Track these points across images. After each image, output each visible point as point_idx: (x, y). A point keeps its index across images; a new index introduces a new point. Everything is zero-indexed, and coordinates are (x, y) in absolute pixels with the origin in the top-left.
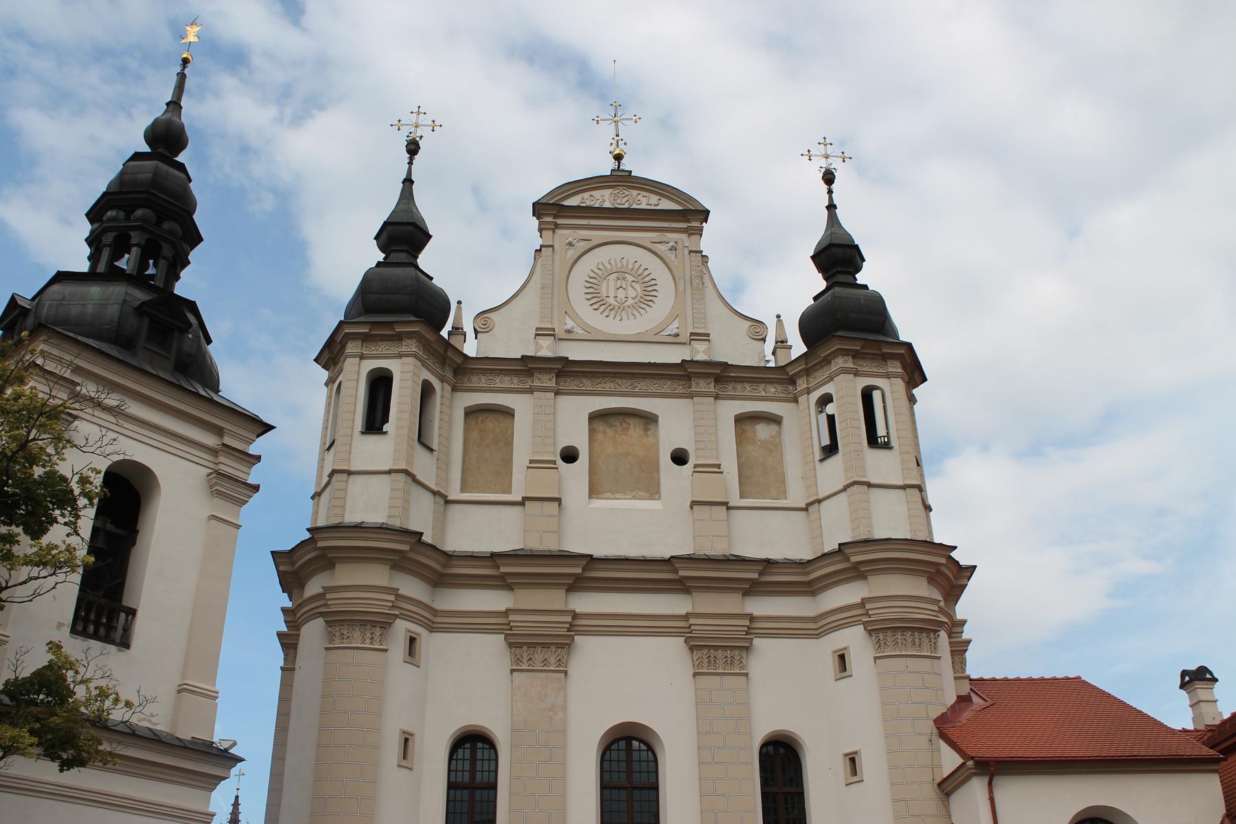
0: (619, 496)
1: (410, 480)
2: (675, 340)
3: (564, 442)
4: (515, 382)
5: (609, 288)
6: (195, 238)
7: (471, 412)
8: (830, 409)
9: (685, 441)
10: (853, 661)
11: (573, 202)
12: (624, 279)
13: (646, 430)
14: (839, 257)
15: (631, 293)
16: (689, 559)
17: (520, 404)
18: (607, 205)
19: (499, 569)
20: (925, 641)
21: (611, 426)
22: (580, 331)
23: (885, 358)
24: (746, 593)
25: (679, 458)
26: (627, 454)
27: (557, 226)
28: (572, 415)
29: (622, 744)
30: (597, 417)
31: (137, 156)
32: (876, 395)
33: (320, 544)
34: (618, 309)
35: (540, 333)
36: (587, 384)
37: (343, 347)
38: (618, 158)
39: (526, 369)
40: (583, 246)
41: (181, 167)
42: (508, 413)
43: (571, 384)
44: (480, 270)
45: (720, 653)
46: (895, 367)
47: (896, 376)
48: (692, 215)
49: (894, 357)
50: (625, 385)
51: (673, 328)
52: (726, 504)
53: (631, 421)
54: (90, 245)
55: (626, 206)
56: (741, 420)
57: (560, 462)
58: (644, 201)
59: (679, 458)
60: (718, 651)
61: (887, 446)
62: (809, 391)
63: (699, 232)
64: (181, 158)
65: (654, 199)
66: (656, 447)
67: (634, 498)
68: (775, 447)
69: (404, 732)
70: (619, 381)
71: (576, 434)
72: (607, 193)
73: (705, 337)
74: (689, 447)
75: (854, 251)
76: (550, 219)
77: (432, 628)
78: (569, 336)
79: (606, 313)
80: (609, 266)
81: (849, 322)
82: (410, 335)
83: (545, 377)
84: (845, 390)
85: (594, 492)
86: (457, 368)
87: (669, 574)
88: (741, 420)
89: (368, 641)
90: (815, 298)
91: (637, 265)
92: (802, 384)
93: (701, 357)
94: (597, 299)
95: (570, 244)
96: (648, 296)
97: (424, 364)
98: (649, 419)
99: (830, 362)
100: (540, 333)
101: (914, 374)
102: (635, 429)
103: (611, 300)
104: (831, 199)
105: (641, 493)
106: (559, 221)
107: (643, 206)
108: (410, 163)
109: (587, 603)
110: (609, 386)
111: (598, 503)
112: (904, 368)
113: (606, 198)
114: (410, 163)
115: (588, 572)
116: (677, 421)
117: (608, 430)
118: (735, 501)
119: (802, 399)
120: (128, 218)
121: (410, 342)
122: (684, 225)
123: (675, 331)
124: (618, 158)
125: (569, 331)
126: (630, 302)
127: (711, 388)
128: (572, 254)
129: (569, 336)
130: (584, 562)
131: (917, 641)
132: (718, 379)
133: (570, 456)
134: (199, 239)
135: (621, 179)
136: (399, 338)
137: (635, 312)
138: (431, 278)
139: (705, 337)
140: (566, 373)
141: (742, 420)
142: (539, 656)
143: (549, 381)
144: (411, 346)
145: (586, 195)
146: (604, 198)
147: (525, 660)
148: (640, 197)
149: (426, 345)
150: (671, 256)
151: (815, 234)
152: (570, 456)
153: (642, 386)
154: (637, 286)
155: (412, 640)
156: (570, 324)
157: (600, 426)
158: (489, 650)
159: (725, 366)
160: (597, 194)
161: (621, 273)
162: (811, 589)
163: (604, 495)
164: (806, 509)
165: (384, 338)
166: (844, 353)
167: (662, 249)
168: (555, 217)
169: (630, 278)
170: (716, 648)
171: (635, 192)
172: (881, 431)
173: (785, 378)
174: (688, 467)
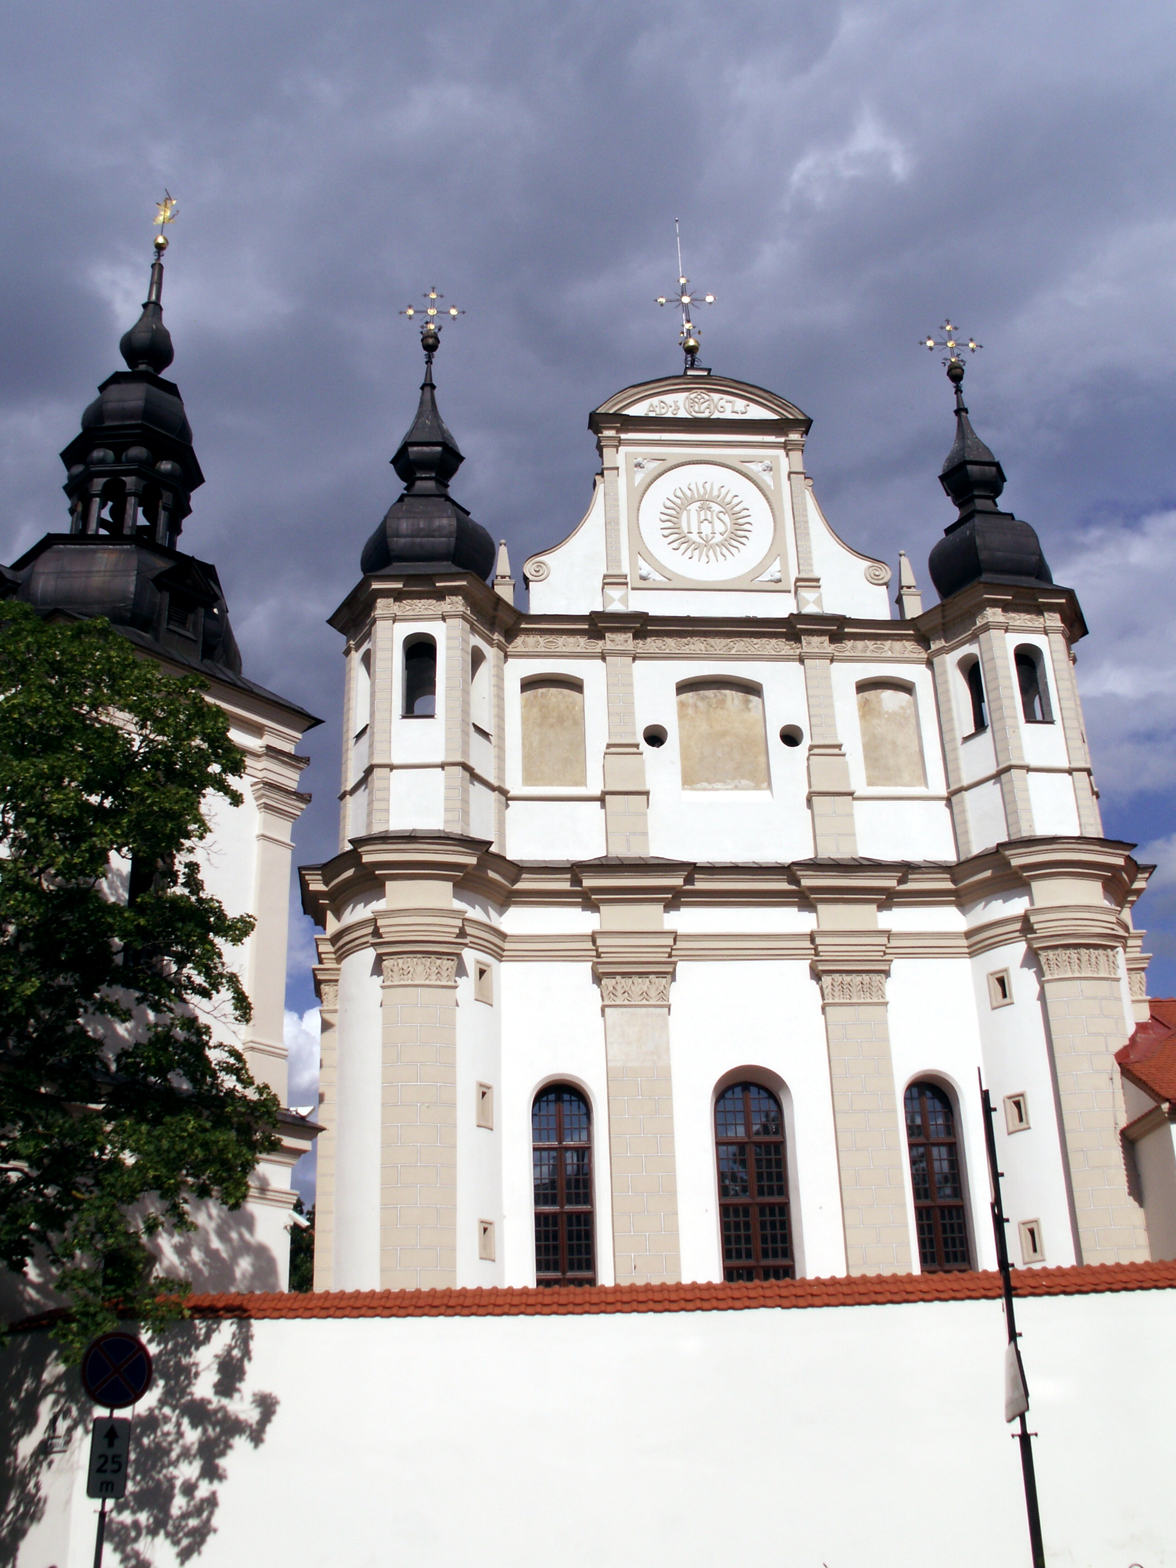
0: (719, 785)
1: (467, 775)
2: (776, 586)
4: (582, 643)
5: (691, 520)
7: (529, 684)
12: (709, 508)
15: (719, 527)
16: (814, 865)
17: (591, 672)
18: (682, 414)
19: (581, 882)
20: (1102, 959)
21: (703, 699)
22: (658, 577)
23: (1039, 610)
25: (791, 737)
26: (724, 734)
27: (620, 442)
28: (653, 684)
30: (684, 687)
31: (117, 378)
33: (366, 859)
35: (611, 581)
36: (671, 644)
37: (371, 606)
40: (652, 466)
41: (171, 389)
42: (575, 685)
43: (651, 645)
45: (857, 979)
46: (1054, 620)
47: (1055, 631)
49: (1052, 608)
50: (719, 644)
51: (774, 570)
52: (851, 794)
55: (706, 415)
56: (864, 686)
57: (644, 746)
58: (728, 407)
59: (791, 737)
60: (847, 975)
64: (166, 375)
69: (481, 1085)
70: (710, 640)
72: (681, 397)
74: (802, 722)
75: (994, 469)
76: (611, 433)
77: (499, 957)
78: (644, 585)
79: (689, 553)
80: (689, 493)
82: (454, 591)
83: (620, 637)
85: (689, 780)
89: (434, 977)
90: (948, 531)
91: (724, 491)
93: (810, 609)
94: (676, 533)
95: (638, 465)
96: (738, 531)
97: (473, 630)
98: (751, 689)
100: (611, 581)
101: (1075, 626)
102: (732, 696)
103: (694, 536)
104: (959, 401)
105: (744, 782)
106: (623, 436)
108: (429, 362)
109: (688, 920)
110: (697, 645)
112: (1063, 621)
113: (681, 404)
114: (429, 362)
115: (687, 883)
117: (700, 704)
120: (118, 460)
121: (454, 598)
122: (782, 440)
123: (778, 576)
126: (718, 538)
127: (829, 648)
128: (640, 476)
131: (1093, 960)
133: (655, 737)
134: (202, 481)
136: (440, 595)
137: (725, 551)
138: (468, 513)
139: (813, 583)
143: (622, 641)
144: (456, 604)
145: (655, 401)
147: (619, 993)
148: (722, 403)
149: (470, 601)
150: (767, 478)
152: (655, 737)
153: (740, 645)
154: (726, 518)
155: (482, 972)
157: (689, 697)
159: (842, 621)
161: (705, 501)
163: (699, 786)
165: (420, 596)
166: (994, 603)
167: (755, 468)
169: (716, 508)
171: (716, 396)
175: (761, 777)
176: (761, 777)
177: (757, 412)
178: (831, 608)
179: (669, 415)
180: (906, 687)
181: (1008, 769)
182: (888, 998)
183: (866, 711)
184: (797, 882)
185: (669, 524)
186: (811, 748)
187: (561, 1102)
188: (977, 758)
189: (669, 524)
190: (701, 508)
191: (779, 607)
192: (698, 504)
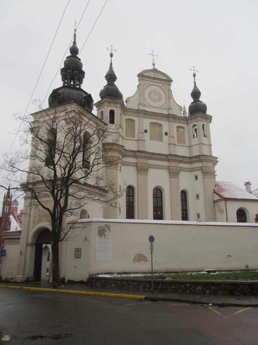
0: (155, 140)
2: (165, 109)
3: (145, 128)
5: (153, 95)
6: (83, 73)
7: (126, 120)
8: (195, 127)
9: (167, 131)
10: (199, 177)
11: (146, 74)
13: (160, 127)
14: (196, 94)
15: (157, 97)
18: (152, 76)
19: (136, 154)
22: (147, 104)
24: (179, 162)
28: (146, 123)
29: (156, 189)
32: (205, 126)
34: (154, 100)
38: (154, 65)
39: (138, 112)
40: (147, 85)
42: (133, 121)
44: (127, 87)
48: (169, 81)
51: (165, 106)
52: (175, 144)
53: (157, 125)
54: (107, 79)
55: (156, 77)
57: (144, 133)
61: (206, 136)
62: (191, 123)
63: (170, 85)
65: (162, 76)
66: (162, 131)
67: (157, 141)
68: (183, 133)
71: (147, 126)
72: (152, 73)
73: (171, 109)
74: (168, 131)
78: (145, 105)
81: (198, 109)
82: (118, 103)
84: (199, 124)
85: (151, 139)
86: (124, 109)
87: (167, 158)
88: (178, 127)
92: (189, 122)
93: (171, 113)
94: (151, 98)
95: (145, 84)
96: (160, 99)
99: (196, 118)
103: (153, 98)
106: (143, 79)
107: (160, 78)
111: (151, 142)
116: (166, 126)
118: (176, 143)
119: (189, 124)
121: (118, 104)
122: (168, 83)
123: (166, 107)
124: (154, 65)
125: (145, 104)
126: (157, 99)
127: (173, 120)
128: (145, 86)
129: (145, 105)
130: (151, 154)
132: (174, 118)
133: (146, 131)
135: (155, 70)
140: (147, 114)
141: (178, 127)
142: (143, 172)
145: (148, 73)
146: (152, 75)
151: (191, 89)
152: (146, 131)
156: (145, 103)
158: (133, 169)
160: (150, 73)
162: (190, 163)
164: (189, 147)
165: (113, 102)
167: (163, 88)
168: (142, 77)
169: (157, 94)
170: (174, 173)
171: (158, 74)
172: (205, 133)
173: (186, 120)
174: (168, 136)
175: (161, 140)
176: (161, 140)
177: (164, 78)
178: (174, 114)
179: (150, 76)
180: (183, 128)
181: (201, 144)
182: (179, 177)
183: (178, 130)
184: (168, 157)
185: (149, 95)
186: (169, 136)
187: (130, 190)
188: (195, 141)
189: (149, 95)
190: (155, 93)
191: (165, 112)
192: (154, 93)
